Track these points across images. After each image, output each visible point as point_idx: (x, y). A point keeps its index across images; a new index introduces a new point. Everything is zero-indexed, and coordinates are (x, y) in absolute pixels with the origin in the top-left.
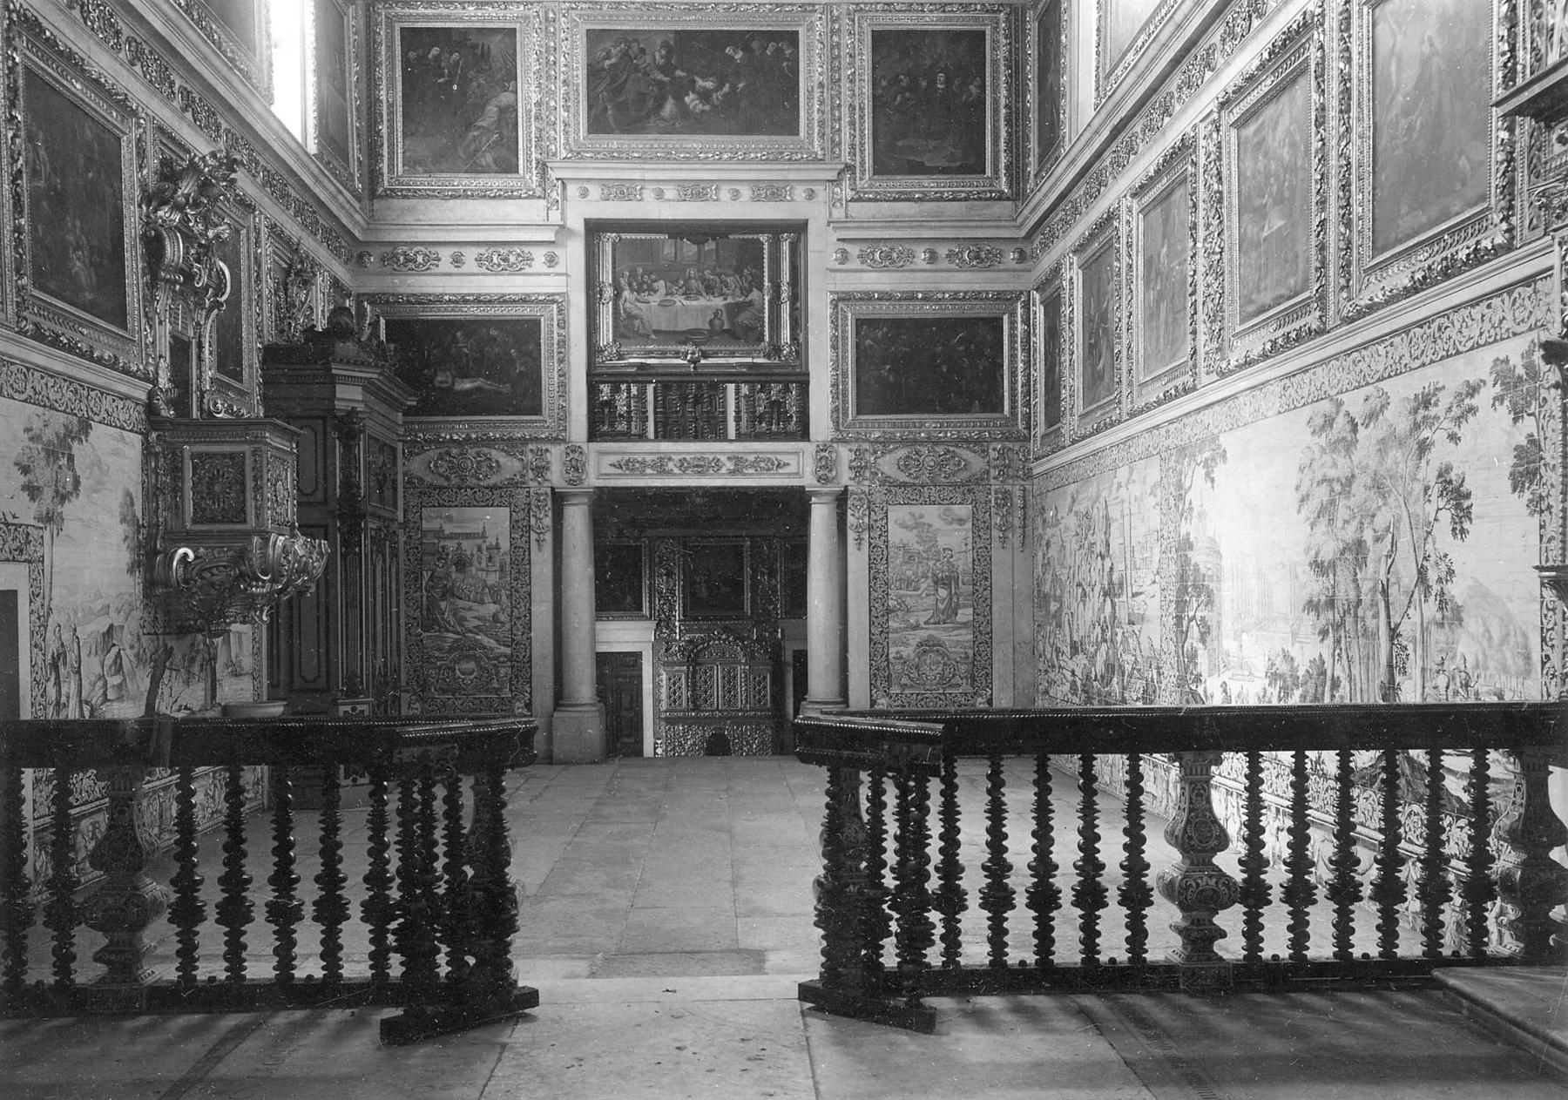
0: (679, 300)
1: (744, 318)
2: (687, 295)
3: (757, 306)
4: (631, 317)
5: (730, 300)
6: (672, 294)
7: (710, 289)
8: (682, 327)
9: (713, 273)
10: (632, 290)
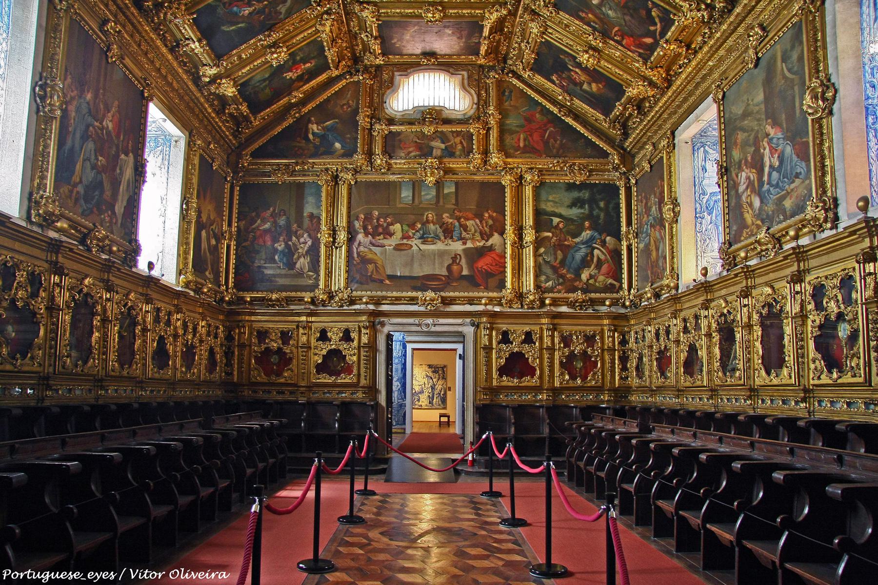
0: (415, 243)
2: (424, 239)
3: (498, 250)
4: (365, 261)
5: (469, 245)
6: (409, 238)
7: (448, 233)
8: (419, 271)
9: (451, 217)
10: (367, 234)
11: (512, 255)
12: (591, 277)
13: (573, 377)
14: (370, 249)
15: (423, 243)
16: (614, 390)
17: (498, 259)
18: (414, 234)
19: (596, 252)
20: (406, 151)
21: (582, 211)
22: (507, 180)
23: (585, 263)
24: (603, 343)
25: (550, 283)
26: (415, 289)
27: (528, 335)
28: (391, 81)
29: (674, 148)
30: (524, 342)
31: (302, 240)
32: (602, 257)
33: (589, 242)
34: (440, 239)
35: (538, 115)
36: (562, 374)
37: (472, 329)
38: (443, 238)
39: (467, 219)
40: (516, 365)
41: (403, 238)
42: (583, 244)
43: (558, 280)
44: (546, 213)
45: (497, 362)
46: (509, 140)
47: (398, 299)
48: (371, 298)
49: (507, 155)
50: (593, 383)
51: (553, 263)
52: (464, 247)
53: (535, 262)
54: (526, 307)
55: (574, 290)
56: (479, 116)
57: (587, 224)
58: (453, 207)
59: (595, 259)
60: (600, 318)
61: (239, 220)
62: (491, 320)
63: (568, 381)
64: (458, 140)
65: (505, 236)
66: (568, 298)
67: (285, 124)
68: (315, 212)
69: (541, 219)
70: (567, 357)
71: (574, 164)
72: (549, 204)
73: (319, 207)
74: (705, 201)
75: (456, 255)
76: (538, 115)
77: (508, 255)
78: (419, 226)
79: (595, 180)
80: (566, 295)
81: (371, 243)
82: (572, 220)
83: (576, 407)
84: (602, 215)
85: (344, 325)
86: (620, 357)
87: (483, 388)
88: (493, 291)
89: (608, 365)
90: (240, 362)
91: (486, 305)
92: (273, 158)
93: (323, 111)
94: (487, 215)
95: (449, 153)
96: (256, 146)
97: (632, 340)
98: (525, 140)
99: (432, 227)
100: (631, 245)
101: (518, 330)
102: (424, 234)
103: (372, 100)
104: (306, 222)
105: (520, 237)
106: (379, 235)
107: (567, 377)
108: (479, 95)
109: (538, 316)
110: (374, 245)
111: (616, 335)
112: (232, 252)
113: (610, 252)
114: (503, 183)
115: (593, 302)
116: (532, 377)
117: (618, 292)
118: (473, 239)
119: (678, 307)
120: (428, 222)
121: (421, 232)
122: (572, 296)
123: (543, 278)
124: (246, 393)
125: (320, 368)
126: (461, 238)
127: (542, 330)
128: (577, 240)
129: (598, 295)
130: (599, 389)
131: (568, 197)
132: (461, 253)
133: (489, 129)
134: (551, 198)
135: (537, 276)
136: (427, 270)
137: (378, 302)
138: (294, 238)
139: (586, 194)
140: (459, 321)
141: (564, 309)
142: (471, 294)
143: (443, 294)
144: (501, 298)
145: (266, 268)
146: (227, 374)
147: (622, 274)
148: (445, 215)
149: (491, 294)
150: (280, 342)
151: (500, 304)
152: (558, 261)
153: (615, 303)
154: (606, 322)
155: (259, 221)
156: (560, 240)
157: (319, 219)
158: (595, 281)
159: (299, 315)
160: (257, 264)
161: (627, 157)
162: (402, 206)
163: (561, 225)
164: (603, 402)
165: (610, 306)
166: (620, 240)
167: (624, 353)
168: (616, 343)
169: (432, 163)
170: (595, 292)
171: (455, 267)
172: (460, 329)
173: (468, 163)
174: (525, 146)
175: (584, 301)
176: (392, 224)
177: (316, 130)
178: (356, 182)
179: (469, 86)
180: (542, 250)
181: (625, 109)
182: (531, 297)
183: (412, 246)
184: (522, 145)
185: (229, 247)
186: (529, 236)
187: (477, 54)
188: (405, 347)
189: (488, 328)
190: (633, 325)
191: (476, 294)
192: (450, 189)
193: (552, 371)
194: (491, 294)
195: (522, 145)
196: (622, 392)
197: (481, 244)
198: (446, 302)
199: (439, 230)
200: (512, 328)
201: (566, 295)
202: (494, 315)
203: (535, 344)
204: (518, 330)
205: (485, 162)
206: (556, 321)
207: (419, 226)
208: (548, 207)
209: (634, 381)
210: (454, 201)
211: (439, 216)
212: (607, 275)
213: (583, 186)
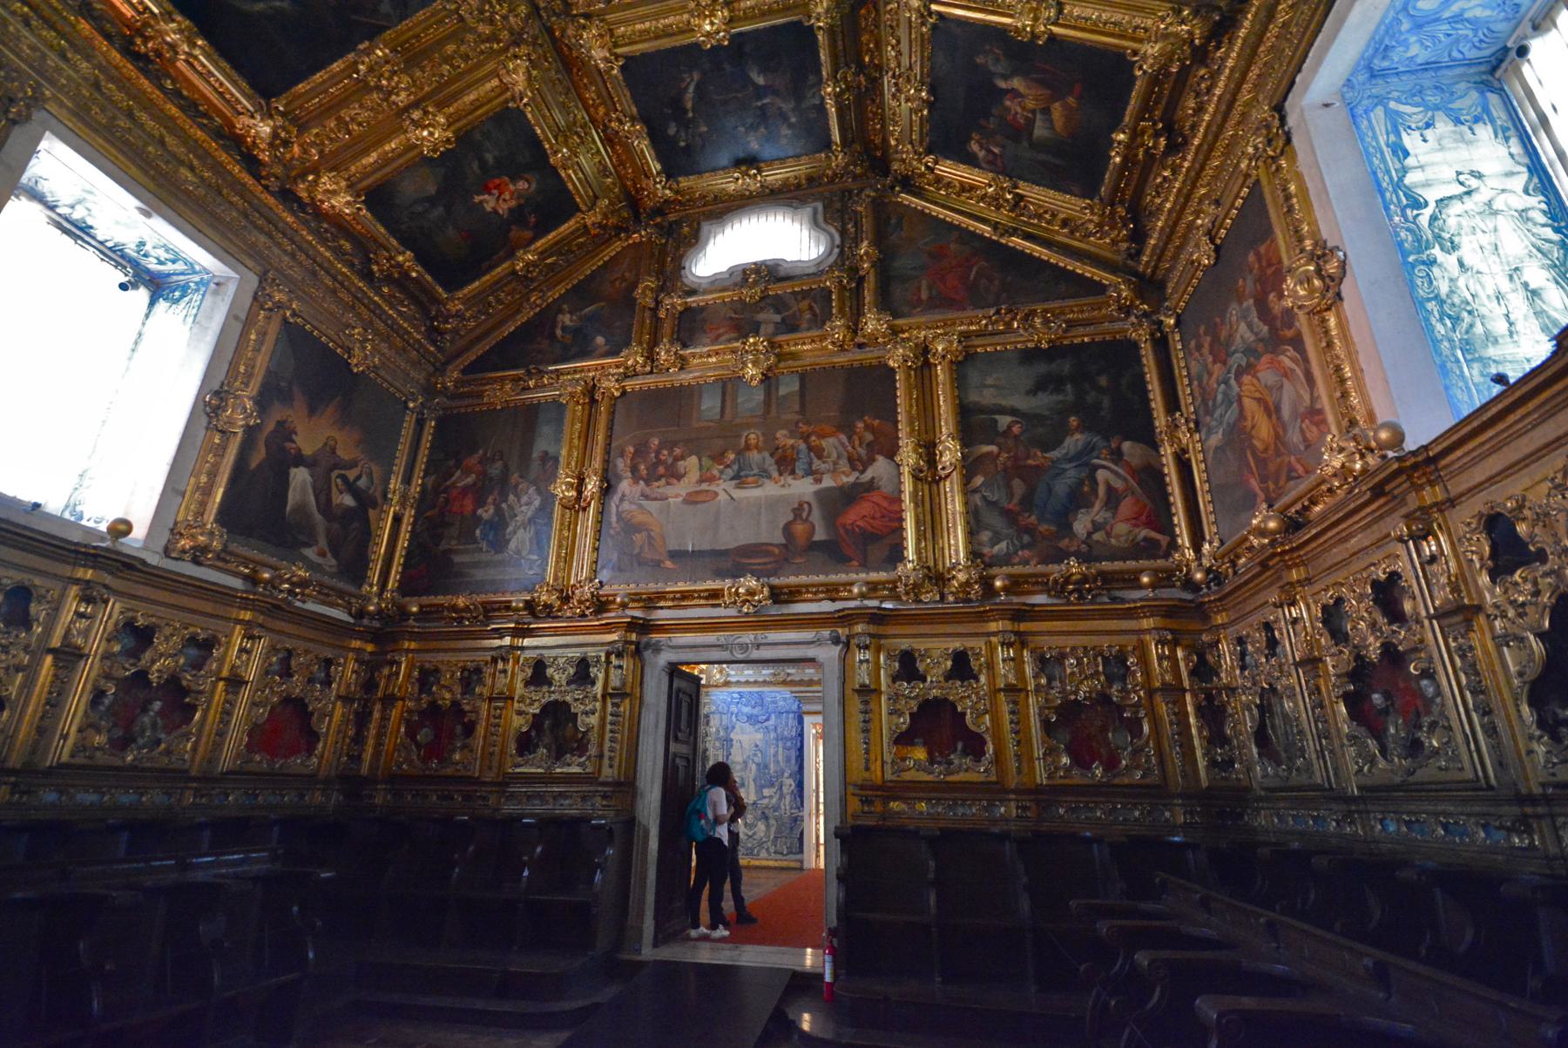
0: (724, 489)
1: (855, 516)
2: (740, 479)
3: (886, 487)
4: (631, 528)
5: (828, 482)
6: (711, 479)
7: (786, 463)
8: (729, 539)
9: (792, 434)
10: (636, 477)
11: (914, 495)
12: (1097, 527)
13: (1081, 760)
14: (641, 506)
15: (738, 487)
16: (1194, 795)
17: (885, 504)
18: (721, 472)
19: (1101, 475)
20: (712, 335)
21: (1060, 397)
22: (896, 357)
23: (1078, 499)
24: (1147, 673)
25: (1003, 545)
26: (720, 574)
27: (960, 658)
29: (1288, 141)
30: (949, 676)
31: (524, 499)
32: (1118, 484)
33: (1082, 458)
34: (769, 477)
35: (953, 246)
36: (1050, 752)
37: (836, 651)
38: (775, 474)
39: (822, 436)
40: (936, 725)
41: (701, 481)
42: (1070, 461)
43: (1020, 538)
44: (981, 409)
45: (889, 721)
46: (897, 291)
47: (686, 595)
48: (635, 597)
49: (896, 316)
50: (1139, 774)
51: (1004, 503)
53: (966, 503)
54: (951, 598)
55: (1060, 556)
56: (843, 257)
57: (1073, 421)
59: (1102, 490)
60: (1130, 614)
61: (427, 473)
62: (872, 629)
63: (1068, 769)
64: (804, 304)
65: (897, 459)
66: (1046, 575)
67: (521, 319)
68: (552, 450)
69: (971, 424)
70: (1058, 710)
71: (1033, 313)
72: (986, 392)
73: (558, 441)
74: (1424, 220)
75: (801, 505)
76: (953, 246)
77: (906, 497)
78: (732, 456)
79: (1083, 336)
80: (1041, 568)
82: (1036, 416)
83: (1098, 840)
84: (1106, 402)
85: (576, 653)
86: (1199, 709)
87: (862, 787)
88: (877, 570)
89: (1168, 729)
90: (380, 735)
91: (863, 596)
92: (497, 370)
93: (582, 293)
94: (860, 425)
95: (790, 326)
96: (471, 357)
97: (1228, 660)
98: (930, 288)
99: (754, 456)
100: (1185, 451)
101: (936, 650)
102: (740, 469)
103: (663, 264)
104: (535, 466)
105: (932, 461)
106: (658, 479)
107: (1065, 760)
108: (843, 233)
109: (982, 617)
110: (647, 497)
111: (1180, 654)
112: (406, 528)
113: (1133, 472)
114: (891, 363)
115: (1108, 579)
116: (978, 759)
117: (1167, 555)
119: (1430, 495)
121: (736, 467)
122: (1055, 570)
123: (985, 536)
124: (378, 800)
125: (525, 744)
126: (810, 472)
127: (992, 649)
128: (1055, 454)
129: (1118, 565)
130: (1156, 793)
131: (1025, 376)
133: (861, 280)
134: (990, 381)
135: (971, 534)
137: (651, 601)
138: (511, 497)
139: (1066, 367)
140: (808, 635)
141: (1040, 599)
142: (833, 578)
143: (775, 581)
144: (894, 582)
145: (457, 552)
146: (351, 757)
147: (1170, 515)
148: (781, 434)
149: (874, 576)
150: (458, 689)
151: (897, 598)
152: (1015, 501)
153: (1164, 579)
154: (1147, 623)
155: (458, 473)
156: (1016, 458)
157: (556, 460)
158: (1108, 535)
159: (500, 634)
160: (443, 546)
161: (1150, 287)
163: (1016, 429)
164: (1173, 828)
165: (1153, 586)
166: (1154, 445)
167: (1209, 697)
168: (1185, 674)
169: (755, 344)
170: (1112, 559)
171: (799, 528)
172: (810, 652)
173: (823, 338)
174: (930, 298)
175: (1085, 579)
176: (683, 458)
177: (568, 323)
178: (624, 393)
179: (825, 220)
180: (979, 480)
181: (1135, 134)
182: (962, 577)
183: (716, 494)
184: (924, 296)
185: (397, 520)
186: (950, 453)
187: (827, 145)
188: (801, 722)
189: (866, 647)
190: (1224, 626)
191: (842, 577)
192: (788, 387)
193: (1023, 740)
194: (874, 576)
195: (924, 296)
196: (1225, 802)
197: (851, 479)
198: (777, 596)
200: (920, 645)
201: (1041, 568)
202: (878, 618)
203: (977, 680)
204: (936, 650)
205: (855, 332)
206: (1023, 626)
207: (732, 456)
208: (987, 397)
209: (1261, 772)
210: (797, 407)
211: (770, 437)
212: (1135, 520)
213: (1055, 351)
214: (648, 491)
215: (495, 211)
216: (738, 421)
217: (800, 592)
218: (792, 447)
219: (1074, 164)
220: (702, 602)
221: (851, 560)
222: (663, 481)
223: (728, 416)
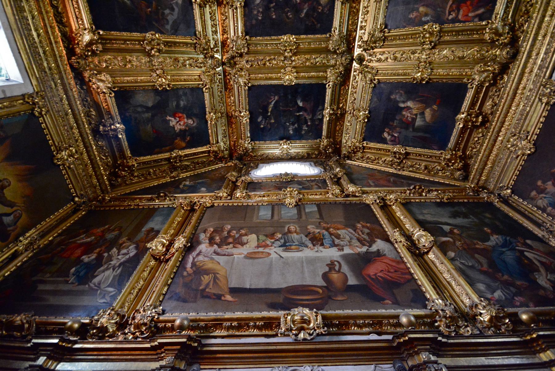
0: (275, 252)
1: (374, 270)
2: (286, 246)
6: (266, 246)
7: (316, 240)
9: (318, 226)
10: (211, 241)
14: (212, 259)
15: (284, 251)
17: (394, 264)
26: (274, 306)
28: (258, 164)
34: (307, 246)
38: (310, 245)
41: (258, 247)
52: (341, 253)
58: (320, 220)
78: (280, 236)
81: (215, 252)
118: (350, 245)
120: (289, 232)
121: (282, 241)
126: (333, 245)
132: (339, 259)
136: (292, 279)
142: (373, 312)
162: (258, 221)
171: (335, 276)
176: (246, 235)
183: (269, 254)
197: (364, 249)
199: (305, 240)
210: (318, 216)
214: (219, 250)
215: (174, 127)
216: (281, 220)
217: (347, 325)
218: (319, 232)
219: (434, 136)
220: (256, 332)
221: (384, 299)
222: (231, 245)
223: (276, 218)
